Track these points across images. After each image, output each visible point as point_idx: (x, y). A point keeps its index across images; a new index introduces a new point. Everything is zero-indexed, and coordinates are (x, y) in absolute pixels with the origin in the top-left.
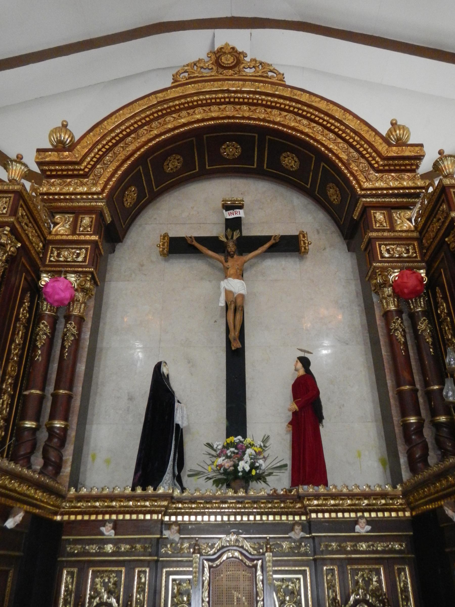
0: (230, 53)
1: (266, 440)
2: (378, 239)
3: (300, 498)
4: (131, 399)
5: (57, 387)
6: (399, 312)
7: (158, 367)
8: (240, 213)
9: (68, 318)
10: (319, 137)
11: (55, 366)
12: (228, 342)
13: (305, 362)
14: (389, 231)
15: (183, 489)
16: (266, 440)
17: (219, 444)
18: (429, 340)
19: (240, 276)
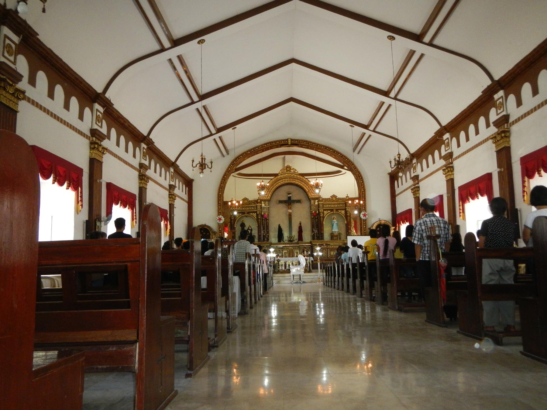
0: (289, 167)
1: (294, 236)
2: (312, 206)
3: (298, 243)
4: (275, 228)
5: (267, 229)
6: (314, 218)
7: (279, 225)
8: (291, 195)
9: (267, 220)
10: (304, 186)
11: (266, 226)
12: (289, 220)
13: (300, 224)
14: (314, 204)
15: (284, 242)
16: (294, 236)
17: (289, 237)
18: (317, 222)
19: (291, 209)
